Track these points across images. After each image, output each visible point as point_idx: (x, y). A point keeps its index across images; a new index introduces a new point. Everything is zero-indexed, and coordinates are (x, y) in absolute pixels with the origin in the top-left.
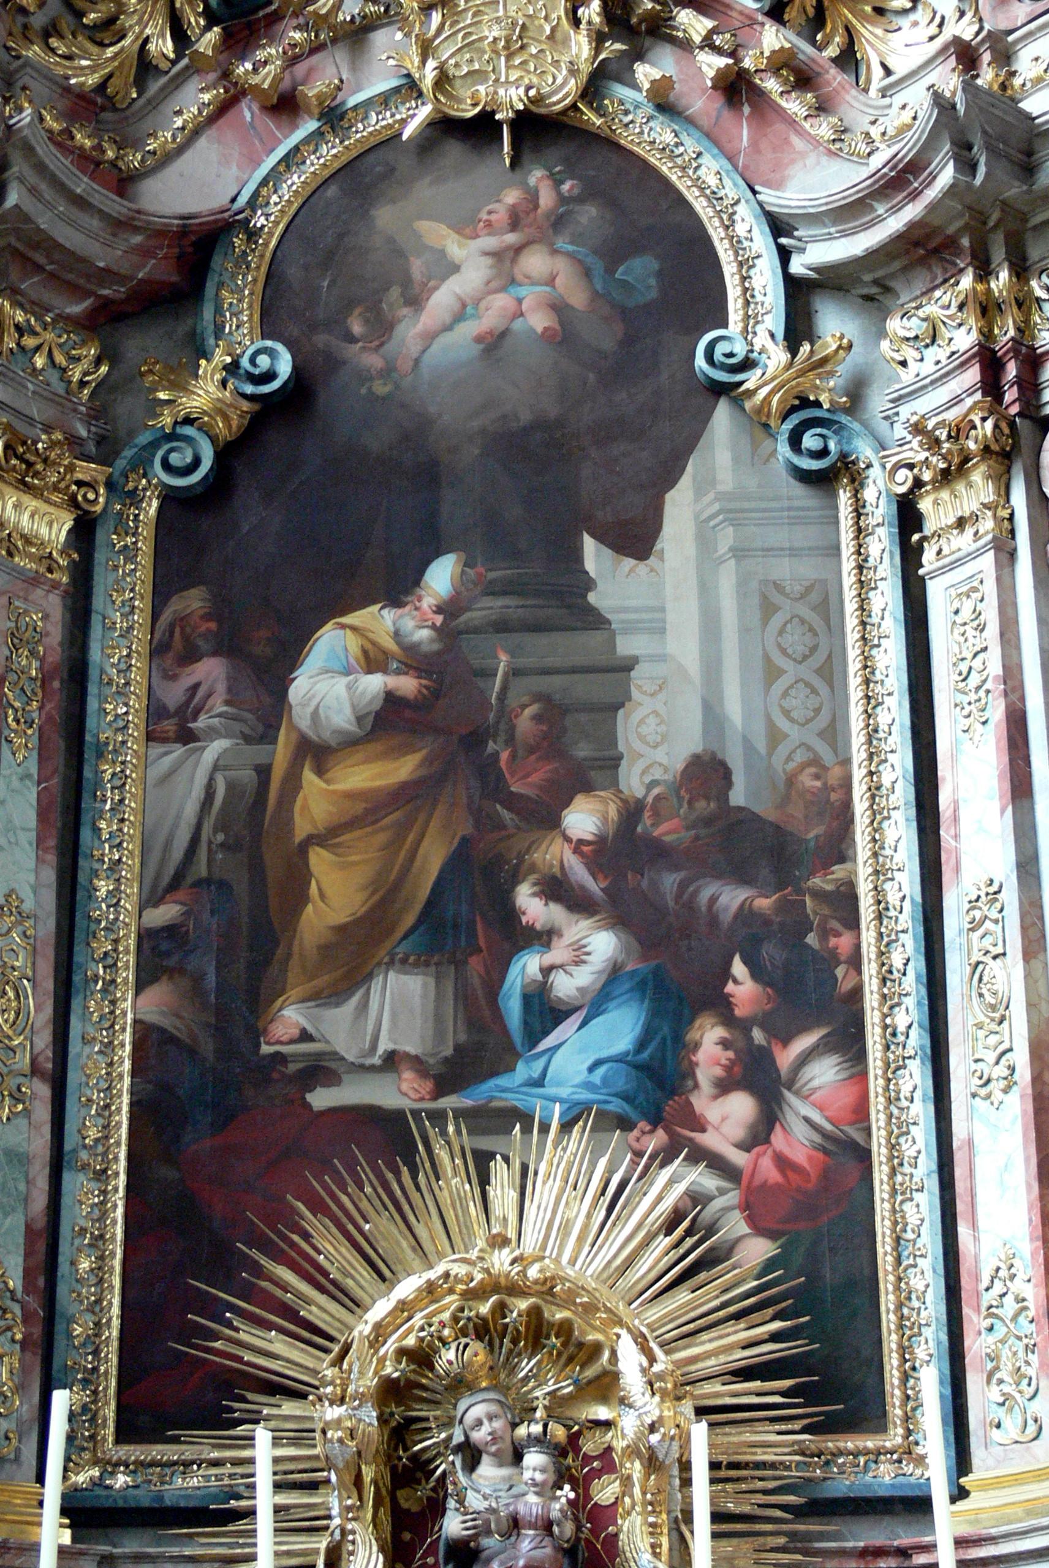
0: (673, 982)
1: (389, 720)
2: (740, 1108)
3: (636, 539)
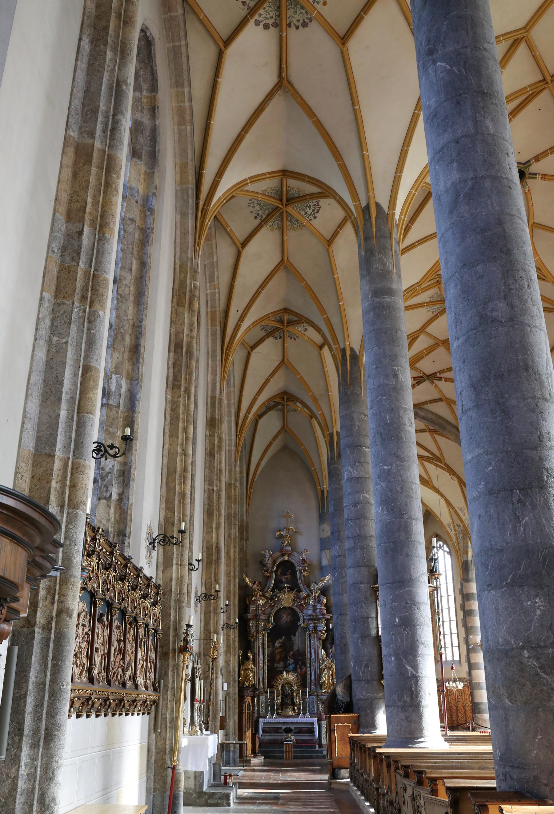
0: (296, 662)
1: (280, 647)
2: (300, 670)
3: (294, 635)
